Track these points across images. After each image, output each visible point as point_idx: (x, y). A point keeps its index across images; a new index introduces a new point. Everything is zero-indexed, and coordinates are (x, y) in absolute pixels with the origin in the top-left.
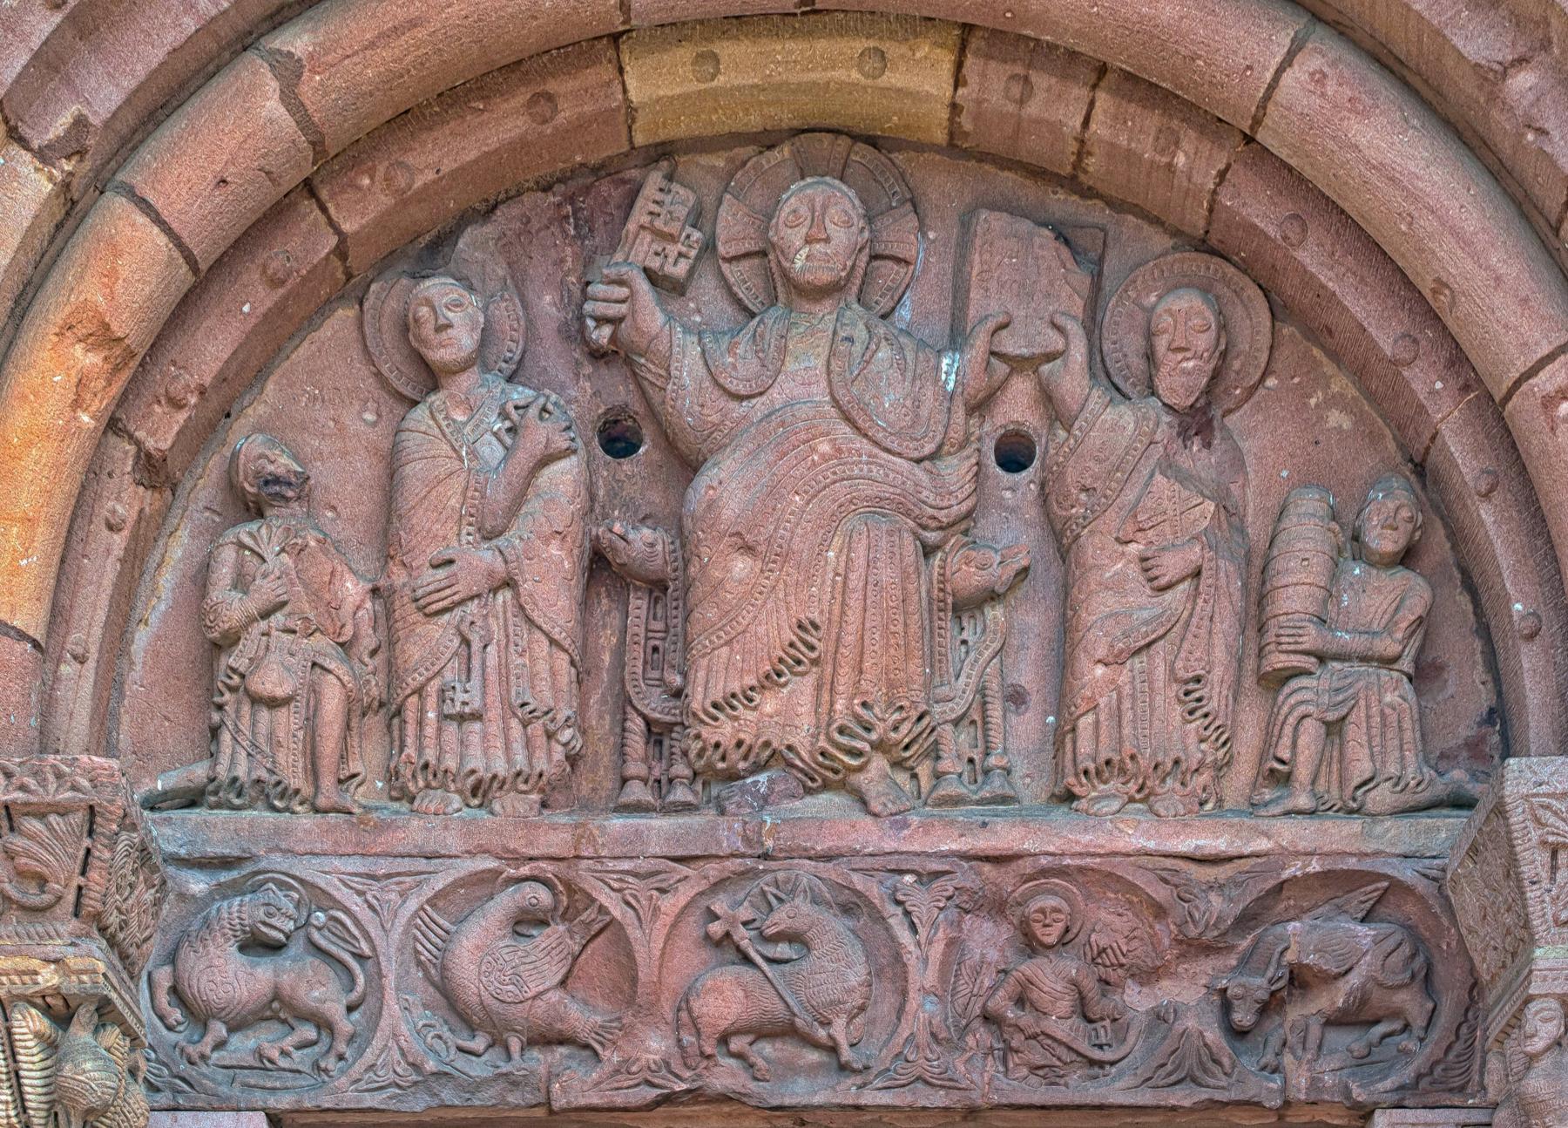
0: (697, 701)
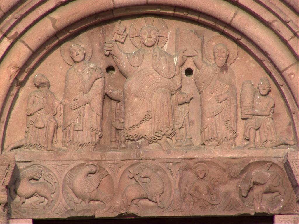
0: (127, 126)
